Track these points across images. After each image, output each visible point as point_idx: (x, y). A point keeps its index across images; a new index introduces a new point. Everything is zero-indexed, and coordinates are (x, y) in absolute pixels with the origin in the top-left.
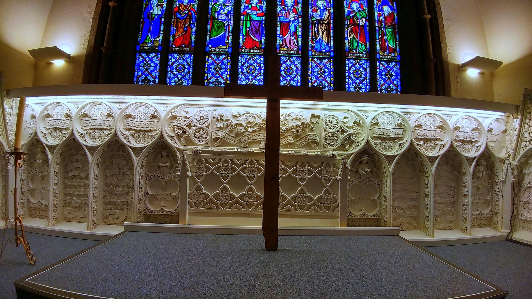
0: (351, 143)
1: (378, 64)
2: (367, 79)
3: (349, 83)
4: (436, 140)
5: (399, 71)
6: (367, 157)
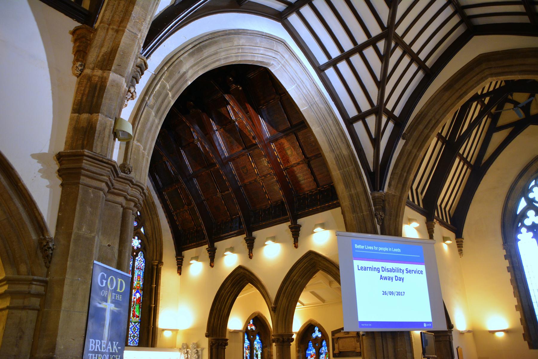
1: (130, 324)
5: (139, 327)
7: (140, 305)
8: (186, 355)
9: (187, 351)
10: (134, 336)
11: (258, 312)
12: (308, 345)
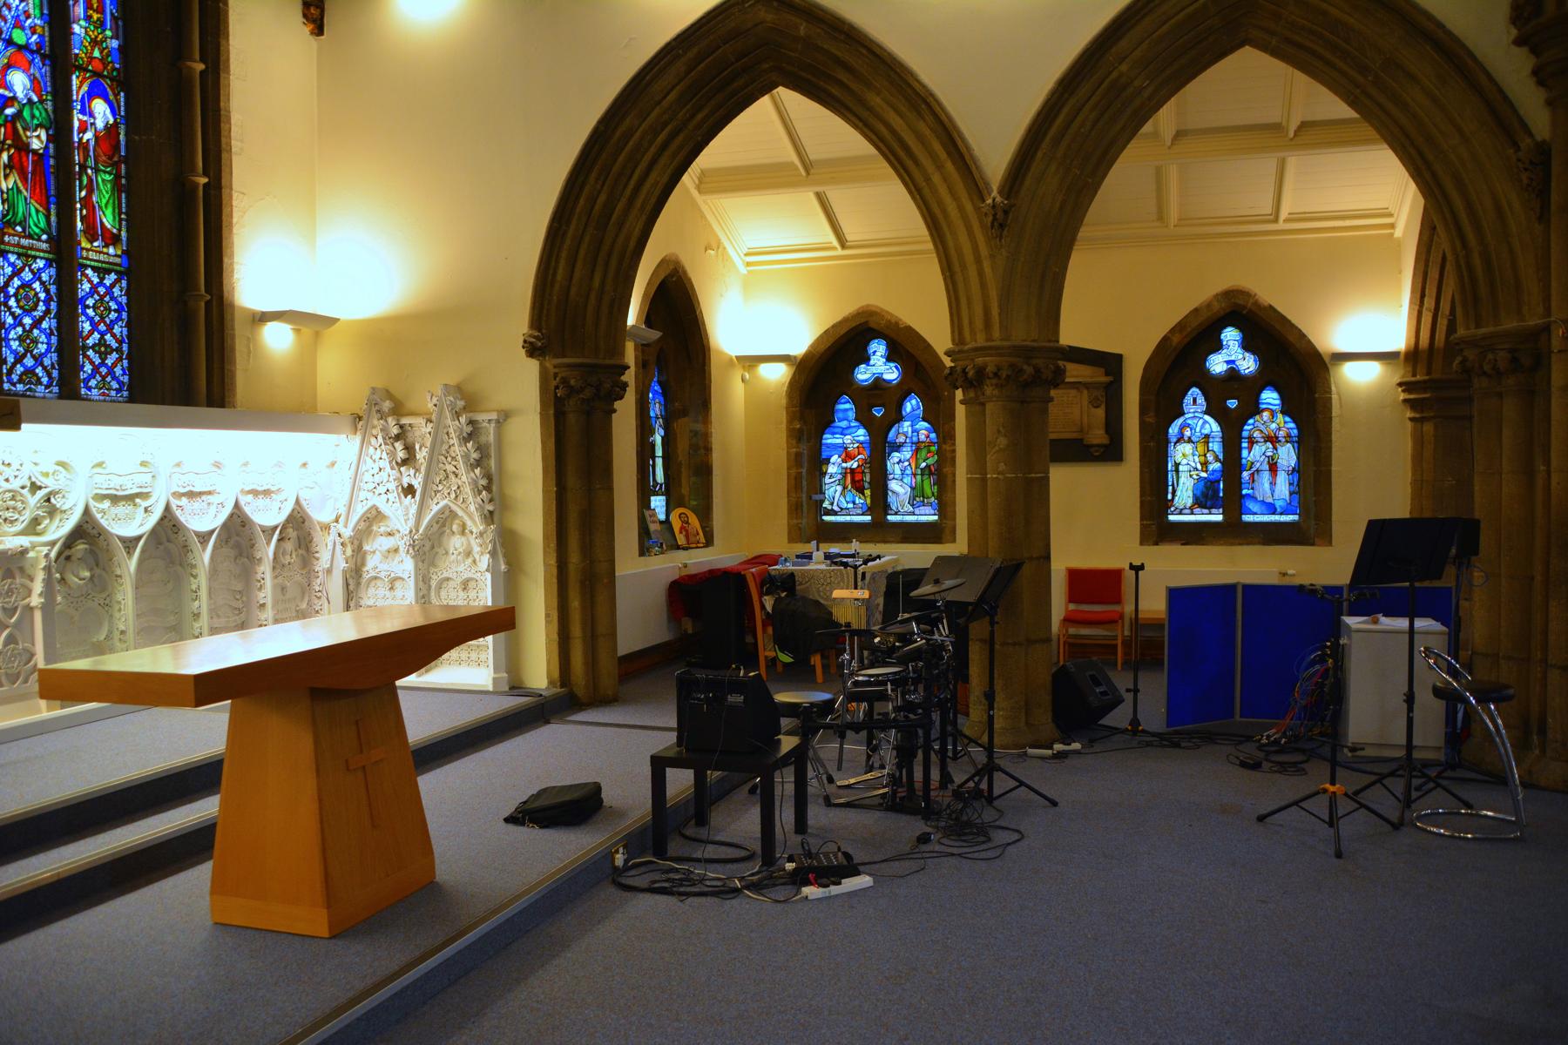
0: (52, 512)
2: (52, 316)
3: (7, 326)
4: (209, 493)
6: (83, 543)
7: (119, 171)
8: (399, 445)
9: (401, 427)
10: (103, 349)
11: (674, 258)
12: (832, 412)
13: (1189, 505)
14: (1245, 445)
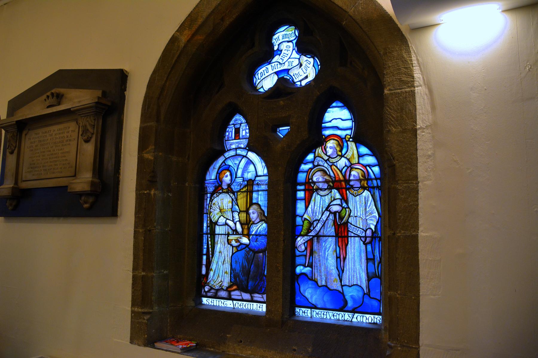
13: (226, 284)
14: (301, 194)
